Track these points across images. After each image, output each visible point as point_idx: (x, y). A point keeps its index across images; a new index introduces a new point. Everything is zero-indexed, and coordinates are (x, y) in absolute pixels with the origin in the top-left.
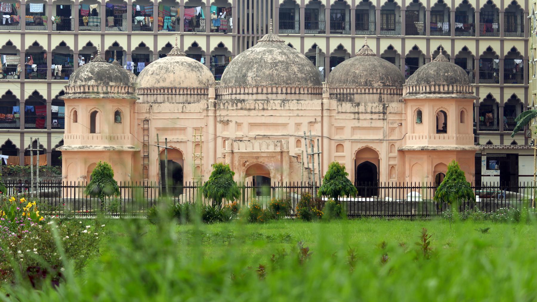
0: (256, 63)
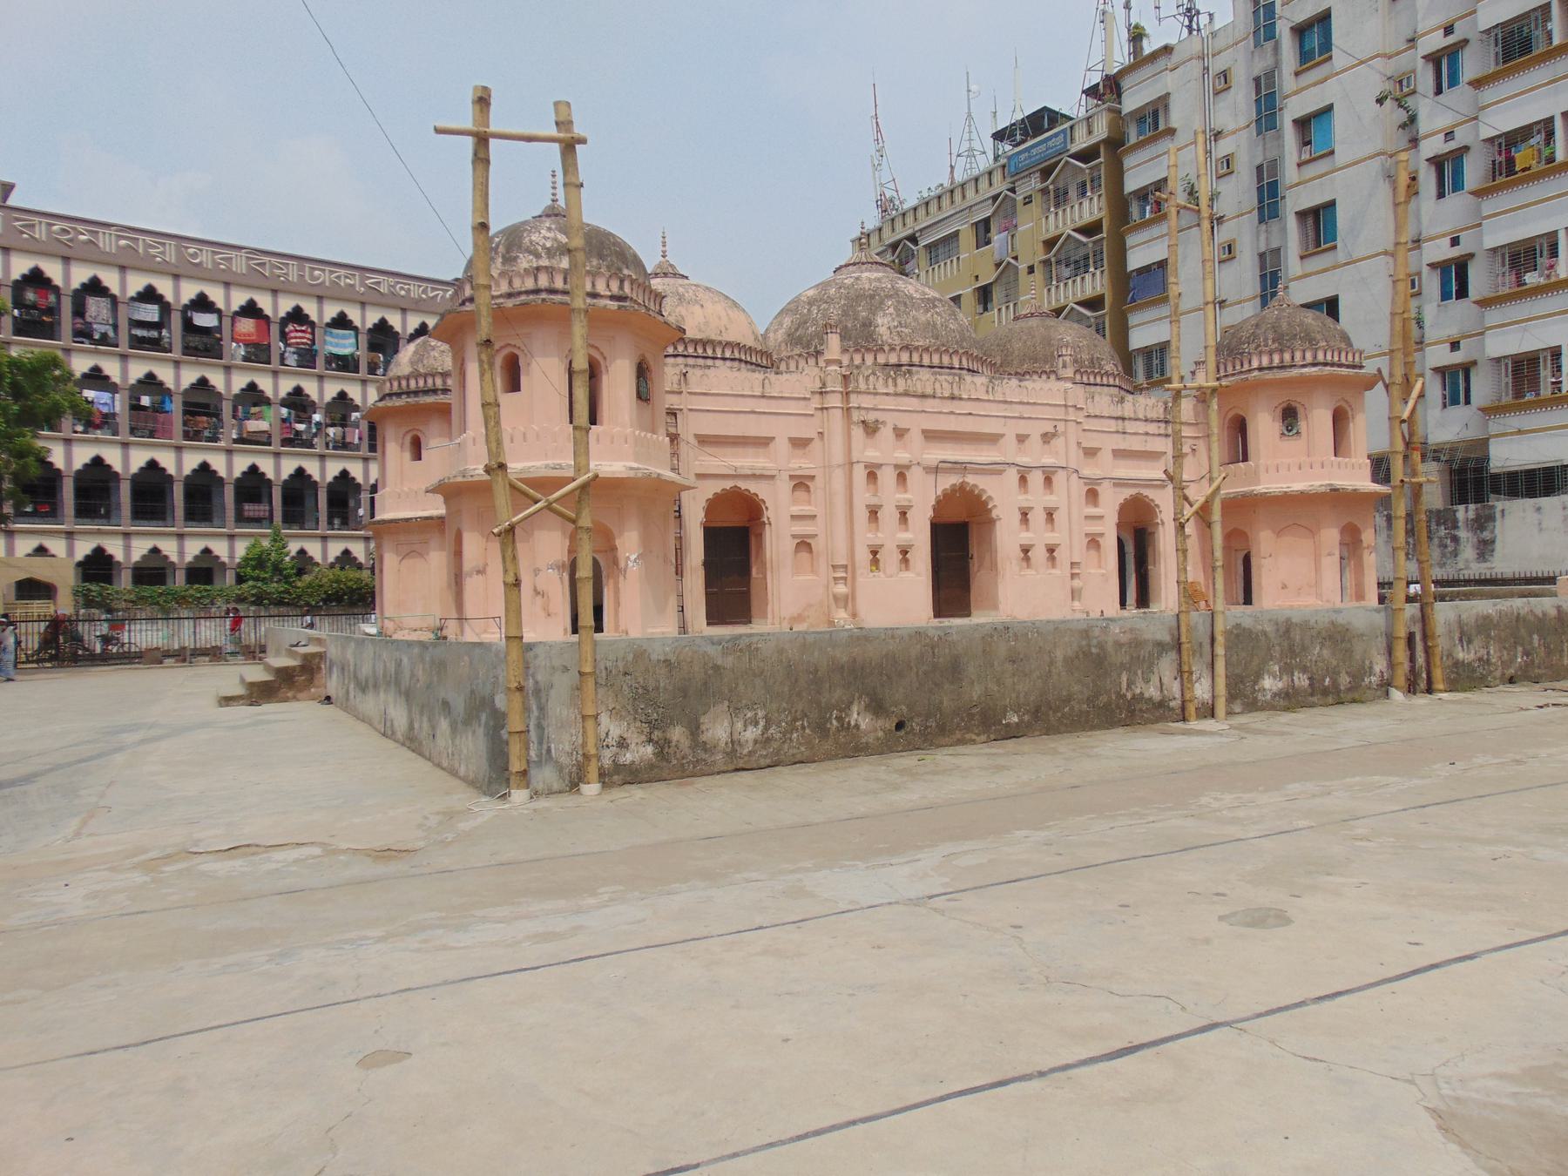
0: (889, 297)
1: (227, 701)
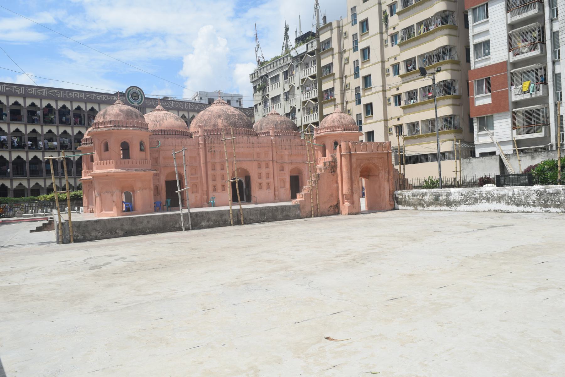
1: (31, 231)
